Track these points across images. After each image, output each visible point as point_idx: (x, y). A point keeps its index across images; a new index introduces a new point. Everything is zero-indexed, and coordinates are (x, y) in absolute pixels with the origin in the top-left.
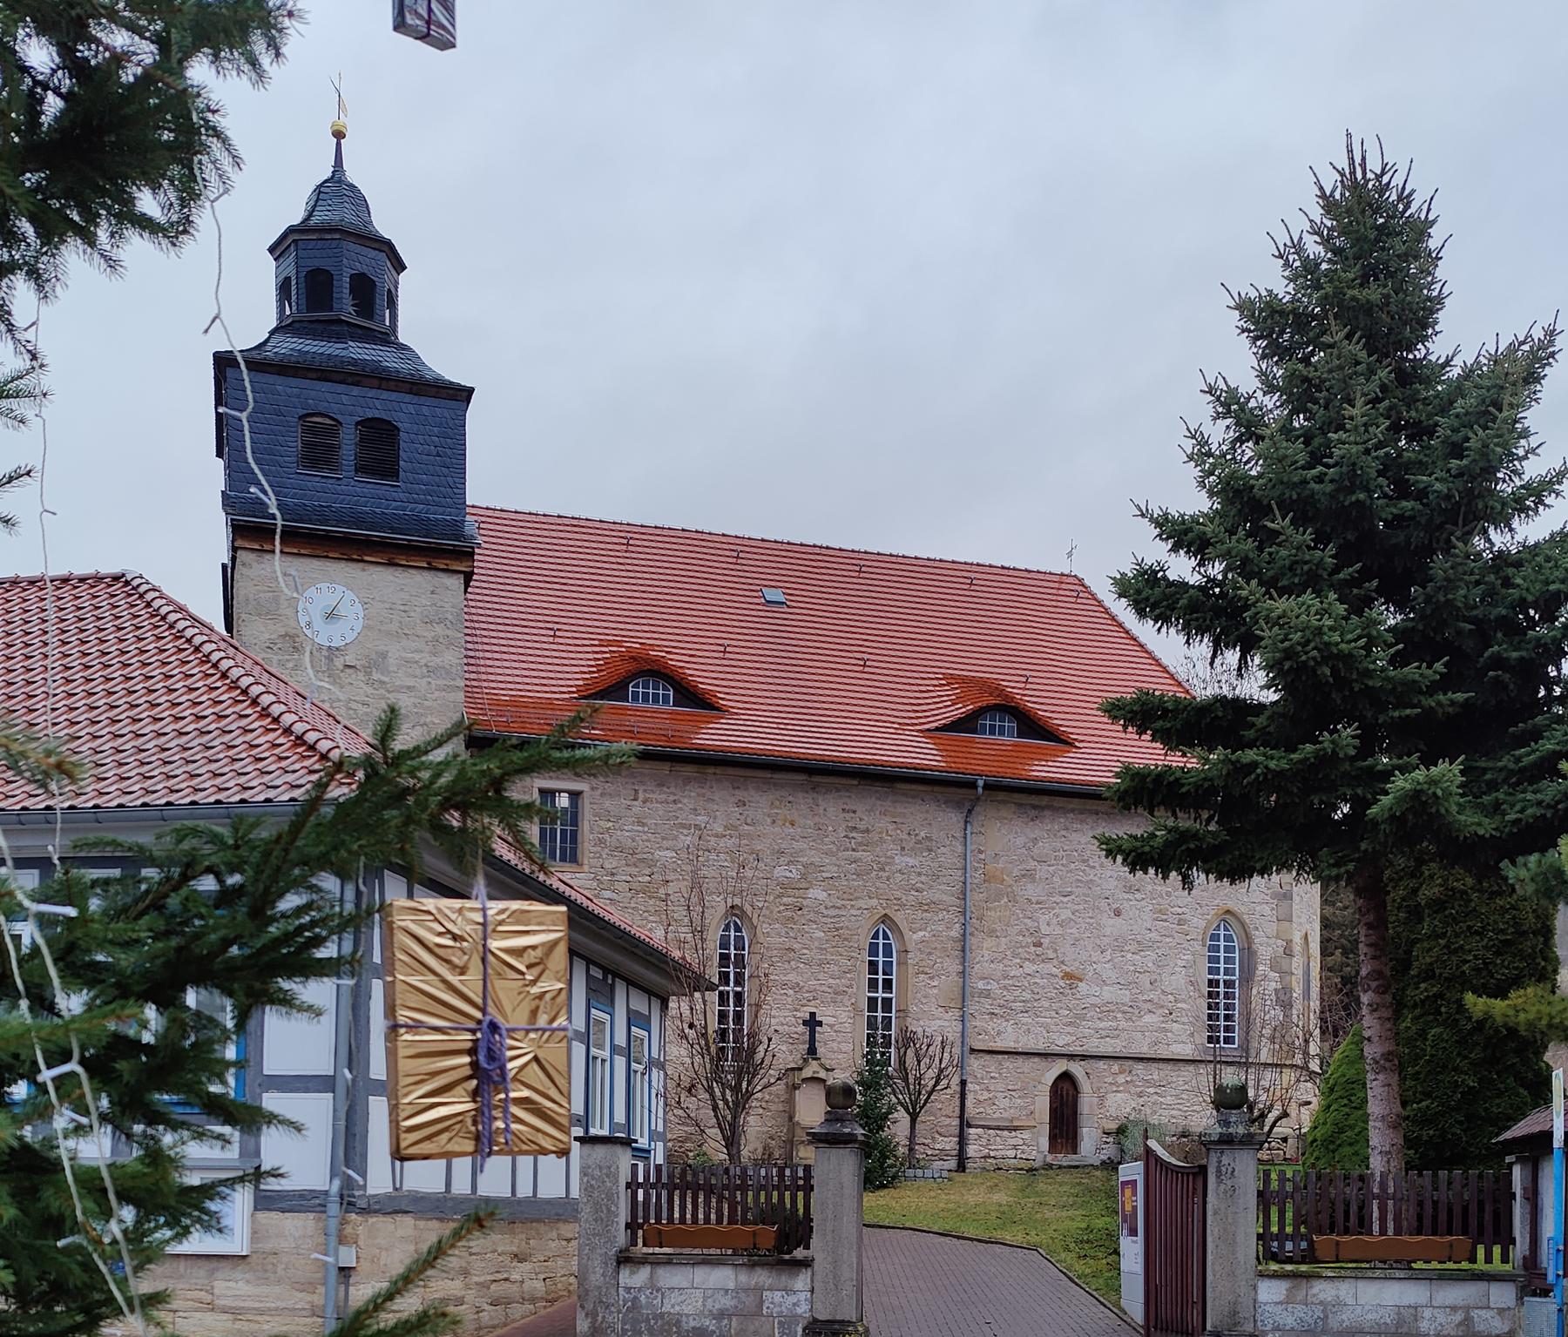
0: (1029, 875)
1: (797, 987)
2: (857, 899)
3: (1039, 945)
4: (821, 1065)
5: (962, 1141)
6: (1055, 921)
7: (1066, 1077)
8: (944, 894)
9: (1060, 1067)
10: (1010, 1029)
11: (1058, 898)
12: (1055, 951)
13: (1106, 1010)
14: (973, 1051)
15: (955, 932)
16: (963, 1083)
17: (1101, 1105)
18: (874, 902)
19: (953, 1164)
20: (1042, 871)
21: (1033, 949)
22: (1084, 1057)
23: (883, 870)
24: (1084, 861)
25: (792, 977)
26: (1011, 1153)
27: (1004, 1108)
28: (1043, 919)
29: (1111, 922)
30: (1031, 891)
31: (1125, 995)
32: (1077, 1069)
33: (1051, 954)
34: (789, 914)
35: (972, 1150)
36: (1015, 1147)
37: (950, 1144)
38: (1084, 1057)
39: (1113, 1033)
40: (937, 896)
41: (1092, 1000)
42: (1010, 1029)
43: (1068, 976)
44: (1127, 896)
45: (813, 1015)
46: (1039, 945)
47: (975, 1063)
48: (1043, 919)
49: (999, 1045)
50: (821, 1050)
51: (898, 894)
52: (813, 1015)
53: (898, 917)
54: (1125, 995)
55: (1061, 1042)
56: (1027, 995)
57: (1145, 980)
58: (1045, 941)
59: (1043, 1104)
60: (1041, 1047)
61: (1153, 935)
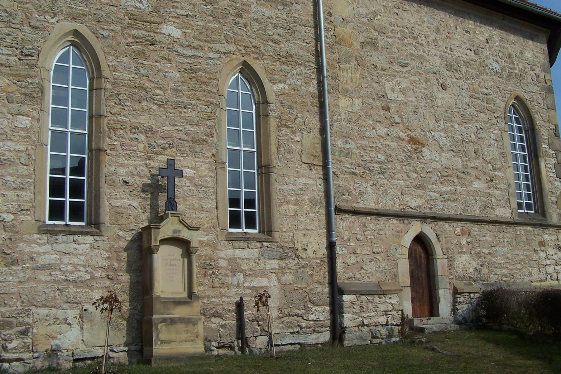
0: (372, 43)
1: (149, 131)
2: (214, 41)
3: (388, 109)
4: (182, 222)
5: (336, 309)
6: (397, 88)
7: (421, 240)
8: (301, 47)
9: (416, 228)
10: (369, 190)
11: (397, 68)
12: (401, 117)
13: (445, 176)
14: (339, 210)
15: (313, 88)
16: (331, 246)
17: (451, 266)
18: (232, 47)
19: (326, 336)
20: (382, 41)
21: (382, 112)
22: (435, 218)
23: (240, 16)
24: (414, 38)
25: (143, 120)
26: (382, 320)
27: (371, 274)
28: (388, 85)
29: (440, 95)
30: (377, 58)
31: (458, 163)
32: (429, 230)
33: (398, 120)
34: (139, 47)
35: (348, 319)
36: (386, 313)
37: (322, 313)
38: (435, 218)
39: (451, 197)
40: (294, 50)
41: (435, 165)
42: (369, 190)
43: (412, 140)
44: (449, 73)
45: (171, 163)
46: (388, 109)
47: (342, 224)
48: (388, 85)
49: (361, 206)
50: (181, 207)
51: (256, 42)
52: (171, 163)
53: (258, 67)
54: (458, 163)
55: (414, 202)
56: (382, 157)
57: (471, 149)
58: (392, 106)
59: (404, 267)
60: (397, 208)
61: (472, 110)
